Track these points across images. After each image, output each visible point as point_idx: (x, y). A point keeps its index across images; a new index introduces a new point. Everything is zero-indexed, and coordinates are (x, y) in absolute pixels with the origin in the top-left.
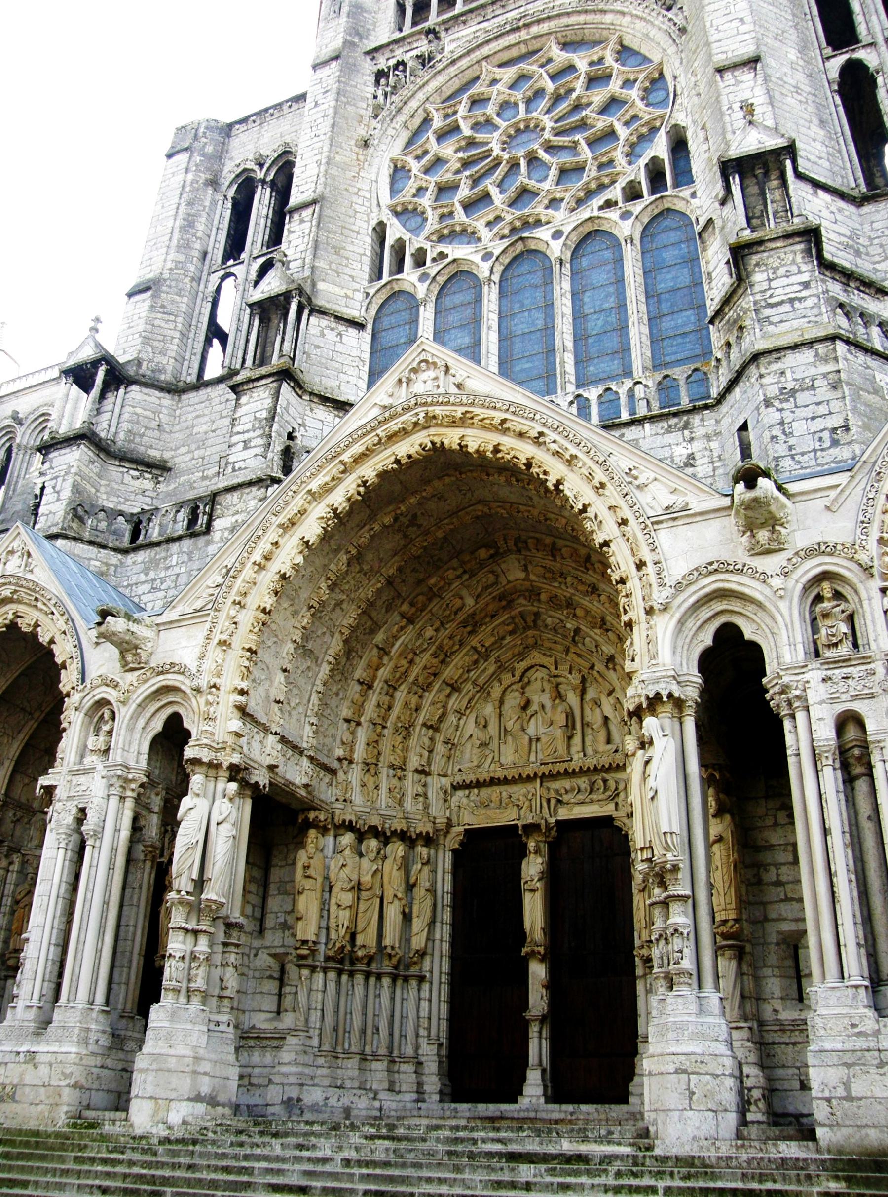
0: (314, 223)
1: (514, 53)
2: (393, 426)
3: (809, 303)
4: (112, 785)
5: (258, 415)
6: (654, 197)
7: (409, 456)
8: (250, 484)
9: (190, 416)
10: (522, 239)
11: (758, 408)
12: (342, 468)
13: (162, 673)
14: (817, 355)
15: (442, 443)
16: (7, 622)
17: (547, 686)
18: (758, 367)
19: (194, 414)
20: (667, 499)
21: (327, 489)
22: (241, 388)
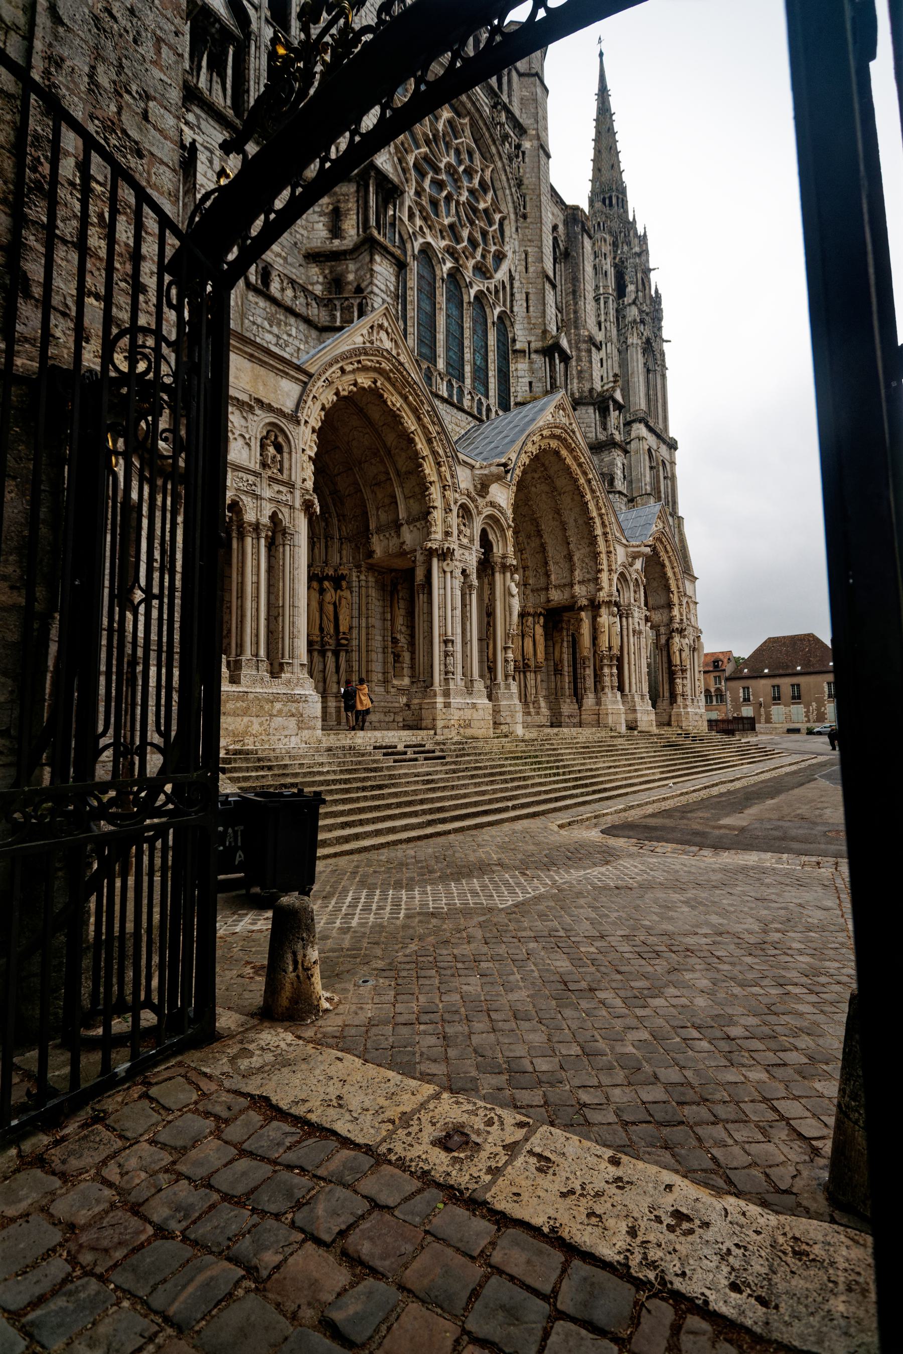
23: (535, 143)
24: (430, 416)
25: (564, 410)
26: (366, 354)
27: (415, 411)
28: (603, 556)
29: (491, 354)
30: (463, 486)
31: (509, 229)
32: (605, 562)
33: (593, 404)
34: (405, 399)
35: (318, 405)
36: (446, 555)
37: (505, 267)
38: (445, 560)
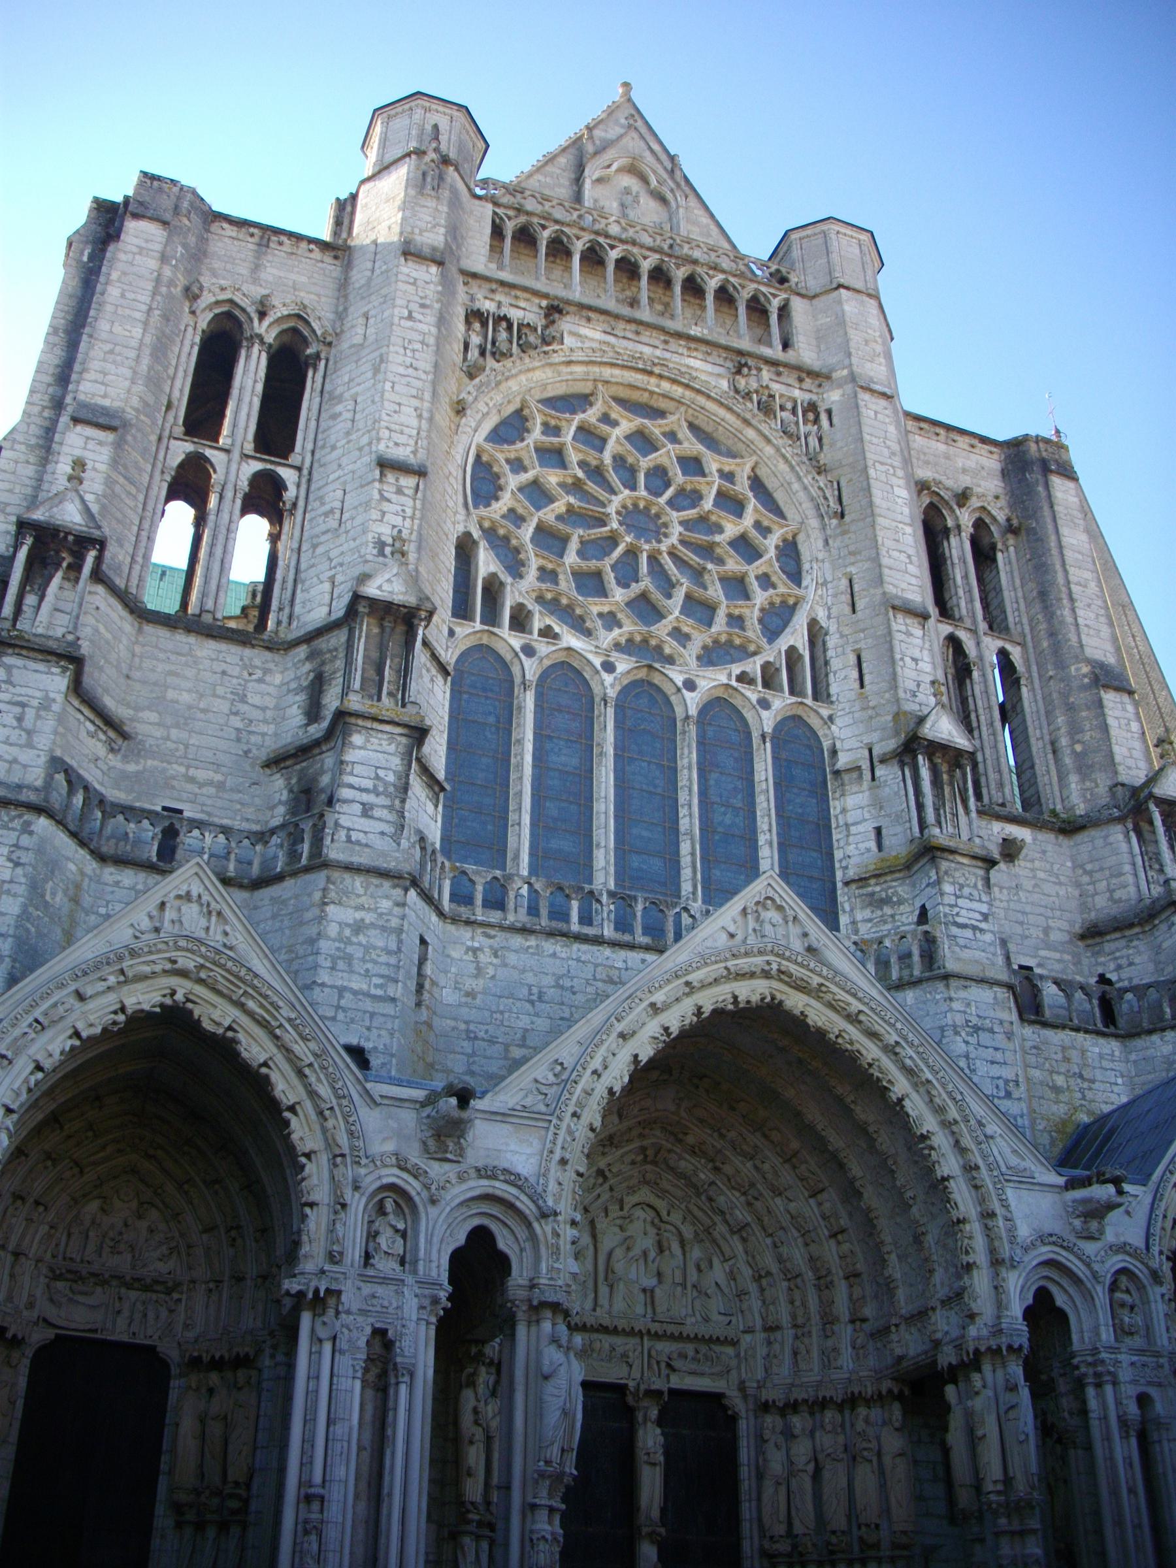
0: (419, 506)
1: (635, 396)
2: (743, 963)
3: (988, 937)
4: (424, 1308)
5: (381, 773)
6: (794, 699)
7: (748, 1002)
8: (384, 874)
9: (161, 667)
10: (650, 667)
11: (942, 1029)
12: (687, 990)
13: (488, 1177)
14: (995, 998)
15: (781, 1002)
16: (168, 1001)
17: (652, 1231)
18: (947, 986)
19: (168, 667)
20: (1014, 1161)
21: (666, 1006)
22: (353, 720)
23: (849, 388)
24: (295, 1027)
25: (780, 908)
26: (133, 953)
27: (263, 1024)
28: (974, 1227)
29: (761, 800)
30: (382, 1146)
31: (811, 548)
32: (979, 1242)
33: (1121, 820)
34: (241, 1006)
35: (23, 1066)
36: (320, 1302)
37: (800, 623)
38: (324, 1314)
